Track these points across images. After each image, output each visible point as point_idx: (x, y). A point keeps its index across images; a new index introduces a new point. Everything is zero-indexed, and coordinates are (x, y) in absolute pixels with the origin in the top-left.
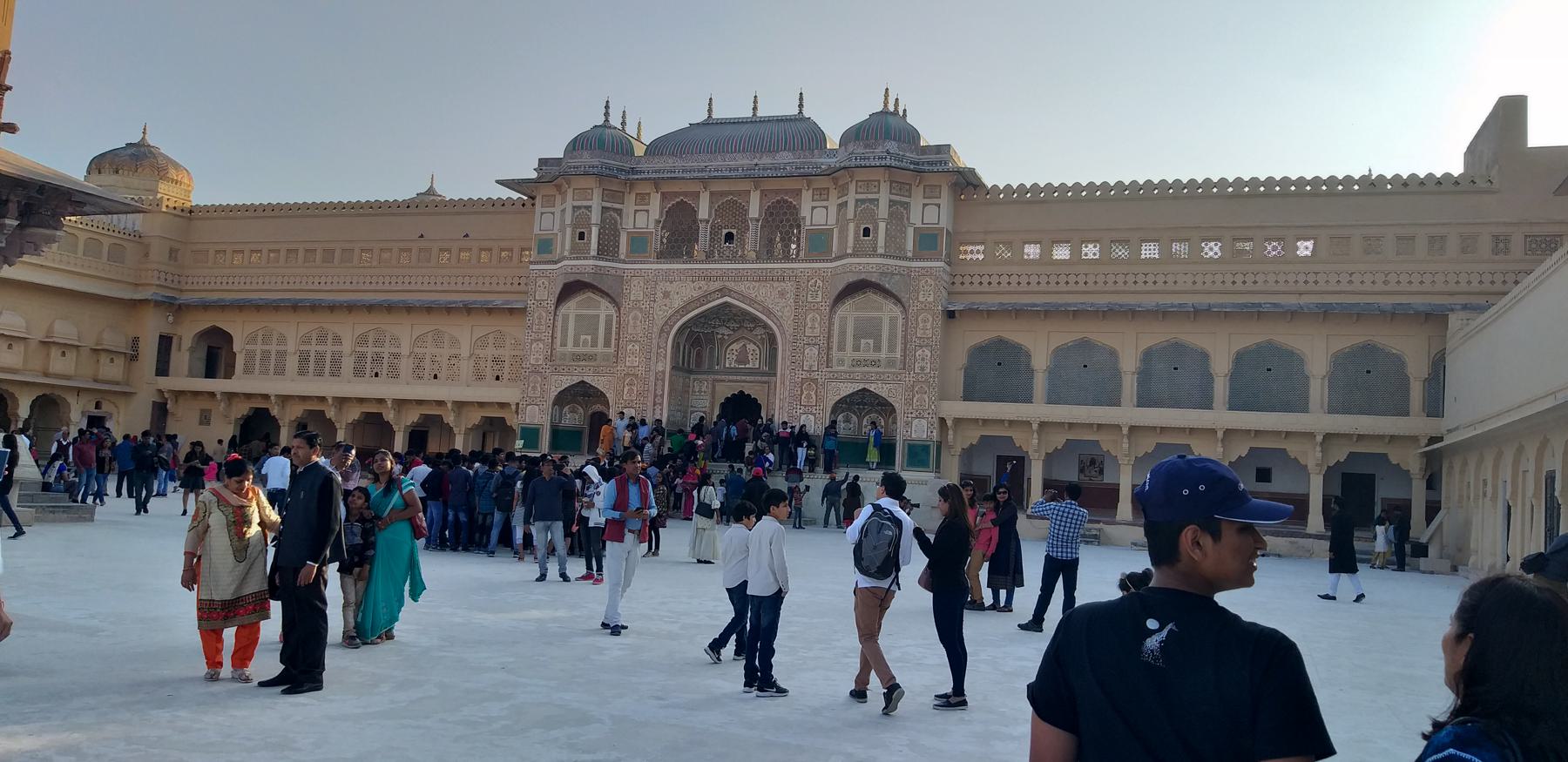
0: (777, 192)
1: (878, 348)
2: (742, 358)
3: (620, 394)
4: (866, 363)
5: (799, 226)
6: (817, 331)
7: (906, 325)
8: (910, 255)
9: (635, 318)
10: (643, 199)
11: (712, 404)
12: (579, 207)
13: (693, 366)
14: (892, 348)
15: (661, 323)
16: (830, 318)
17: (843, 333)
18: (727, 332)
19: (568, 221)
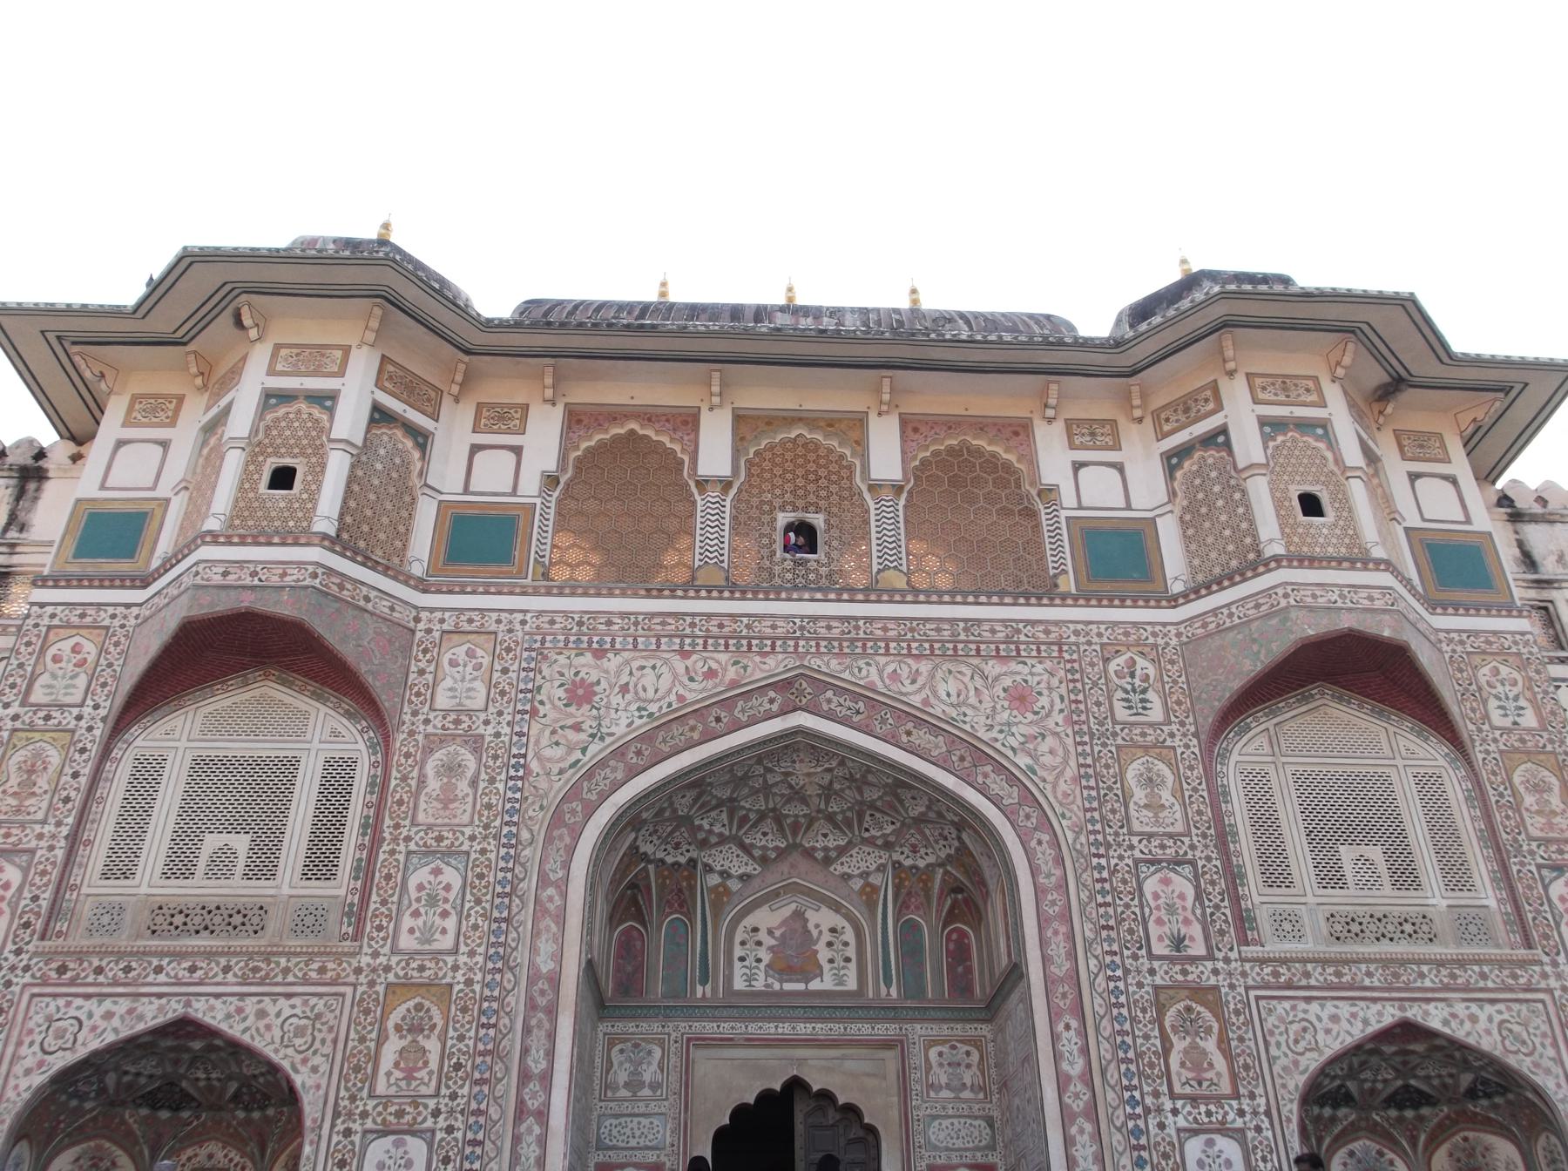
0: (952, 424)
1: (1405, 875)
2: (795, 956)
3: (361, 1068)
4: (1382, 925)
5: (1031, 514)
6: (1174, 819)
7: (1478, 795)
8: (1420, 589)
9: (451, 769)
10: (503, 418)
11: (684, 1130)
12: (286, 397)
13: (609, 988)
14: (1456, 876)
15: (560, 787)
16: (1210, 775)
17: (1266, 824)
18: (738, 864)
19: (241, 423)
